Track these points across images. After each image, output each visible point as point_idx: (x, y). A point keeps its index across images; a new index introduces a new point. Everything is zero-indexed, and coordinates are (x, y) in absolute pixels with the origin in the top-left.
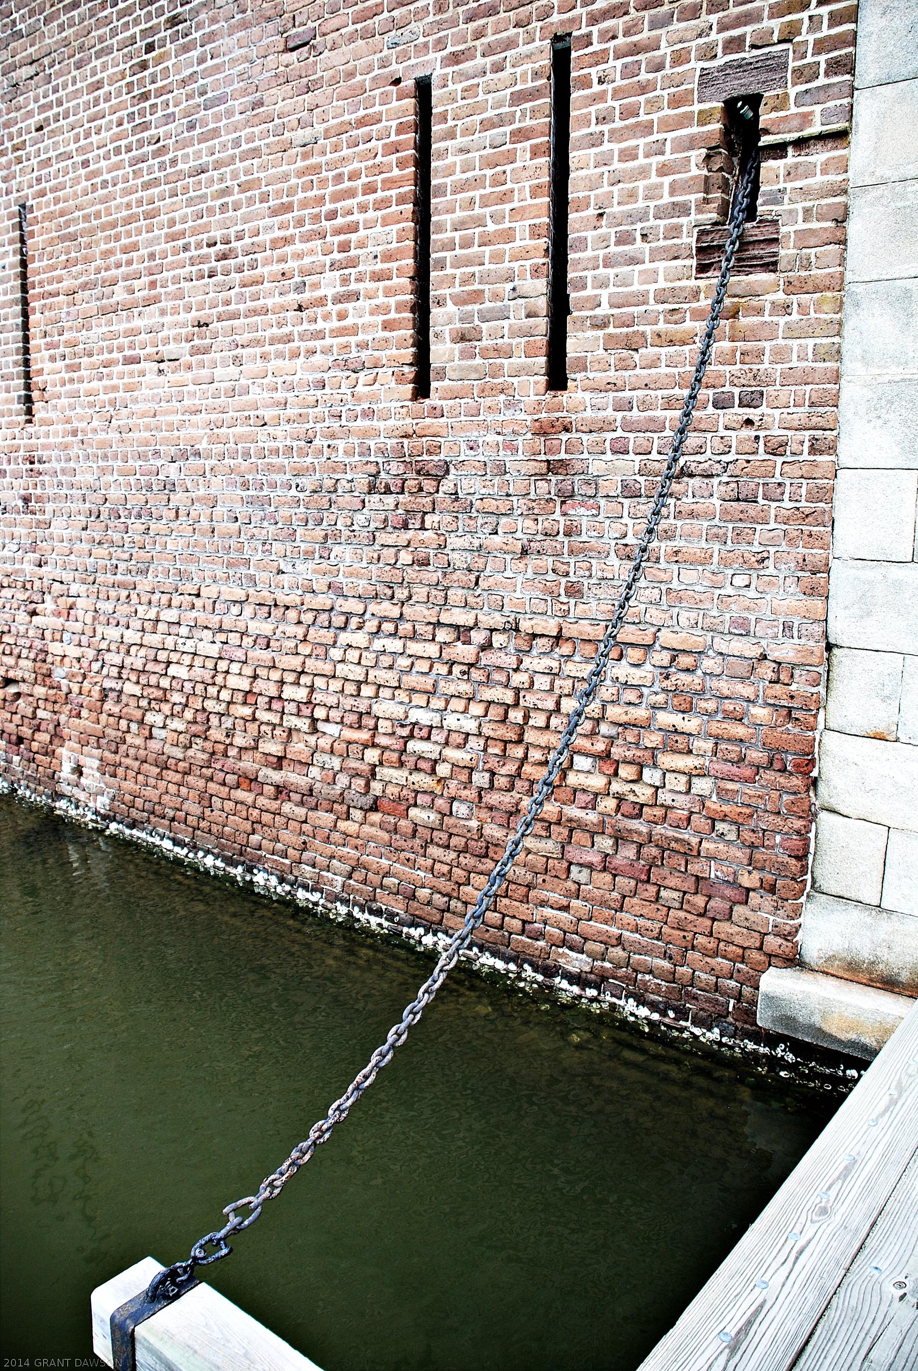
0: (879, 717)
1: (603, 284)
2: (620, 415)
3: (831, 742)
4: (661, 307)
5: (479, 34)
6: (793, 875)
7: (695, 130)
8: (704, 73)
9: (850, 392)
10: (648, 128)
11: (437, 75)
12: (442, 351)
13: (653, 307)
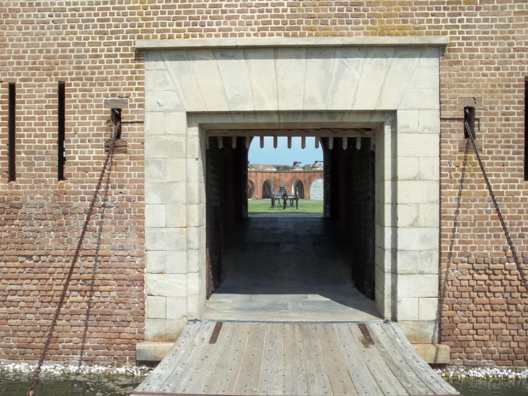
0: (160, 268)
2: (83, 190)
4: (94, 161)
5: (34, 75)
6: (140, 316)
7: (103, 115)
8: (106, 101)
9: (147, 185)
10: (89, 112)
11: (18, 82)
12: (20, 168)
13: (92, 160)
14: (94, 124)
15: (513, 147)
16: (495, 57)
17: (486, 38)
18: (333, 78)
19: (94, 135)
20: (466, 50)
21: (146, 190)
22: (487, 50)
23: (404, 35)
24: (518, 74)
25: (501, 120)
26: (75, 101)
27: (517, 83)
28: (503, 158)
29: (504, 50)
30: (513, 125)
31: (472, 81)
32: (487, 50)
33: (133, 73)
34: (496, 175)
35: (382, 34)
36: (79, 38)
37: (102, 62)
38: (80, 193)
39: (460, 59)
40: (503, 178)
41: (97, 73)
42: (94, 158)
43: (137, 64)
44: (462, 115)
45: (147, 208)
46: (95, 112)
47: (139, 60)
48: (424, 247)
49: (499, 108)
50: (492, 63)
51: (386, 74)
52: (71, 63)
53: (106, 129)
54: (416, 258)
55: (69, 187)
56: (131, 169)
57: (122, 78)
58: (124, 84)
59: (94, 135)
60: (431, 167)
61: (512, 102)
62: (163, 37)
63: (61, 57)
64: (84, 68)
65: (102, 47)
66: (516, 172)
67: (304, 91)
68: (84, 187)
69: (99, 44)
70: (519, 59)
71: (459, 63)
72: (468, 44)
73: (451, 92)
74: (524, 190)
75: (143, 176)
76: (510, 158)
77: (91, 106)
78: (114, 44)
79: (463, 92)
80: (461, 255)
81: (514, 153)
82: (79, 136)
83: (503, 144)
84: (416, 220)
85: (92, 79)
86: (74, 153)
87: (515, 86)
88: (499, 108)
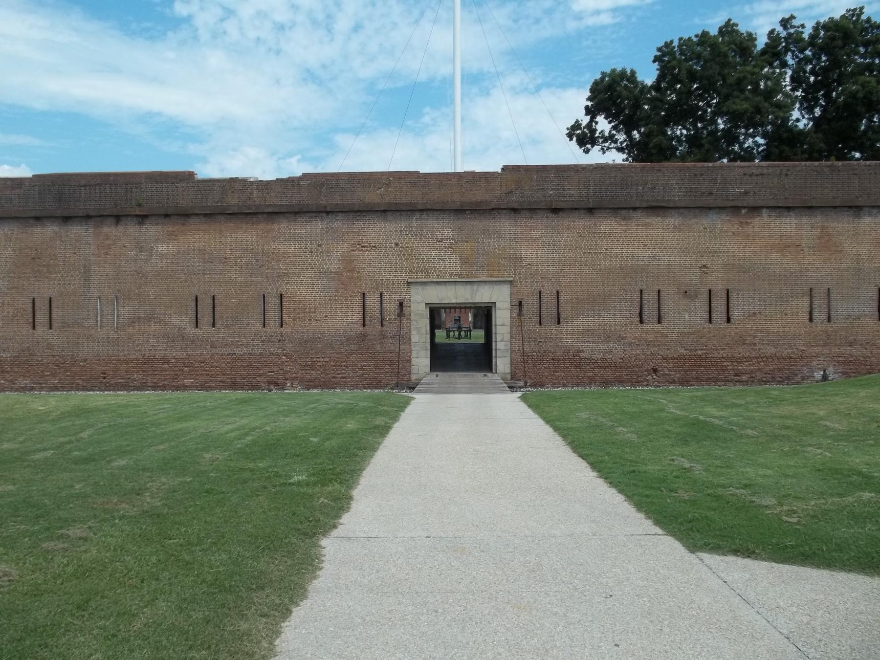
6: (410, 373)
12: (367, 322)
60: (508, 321)
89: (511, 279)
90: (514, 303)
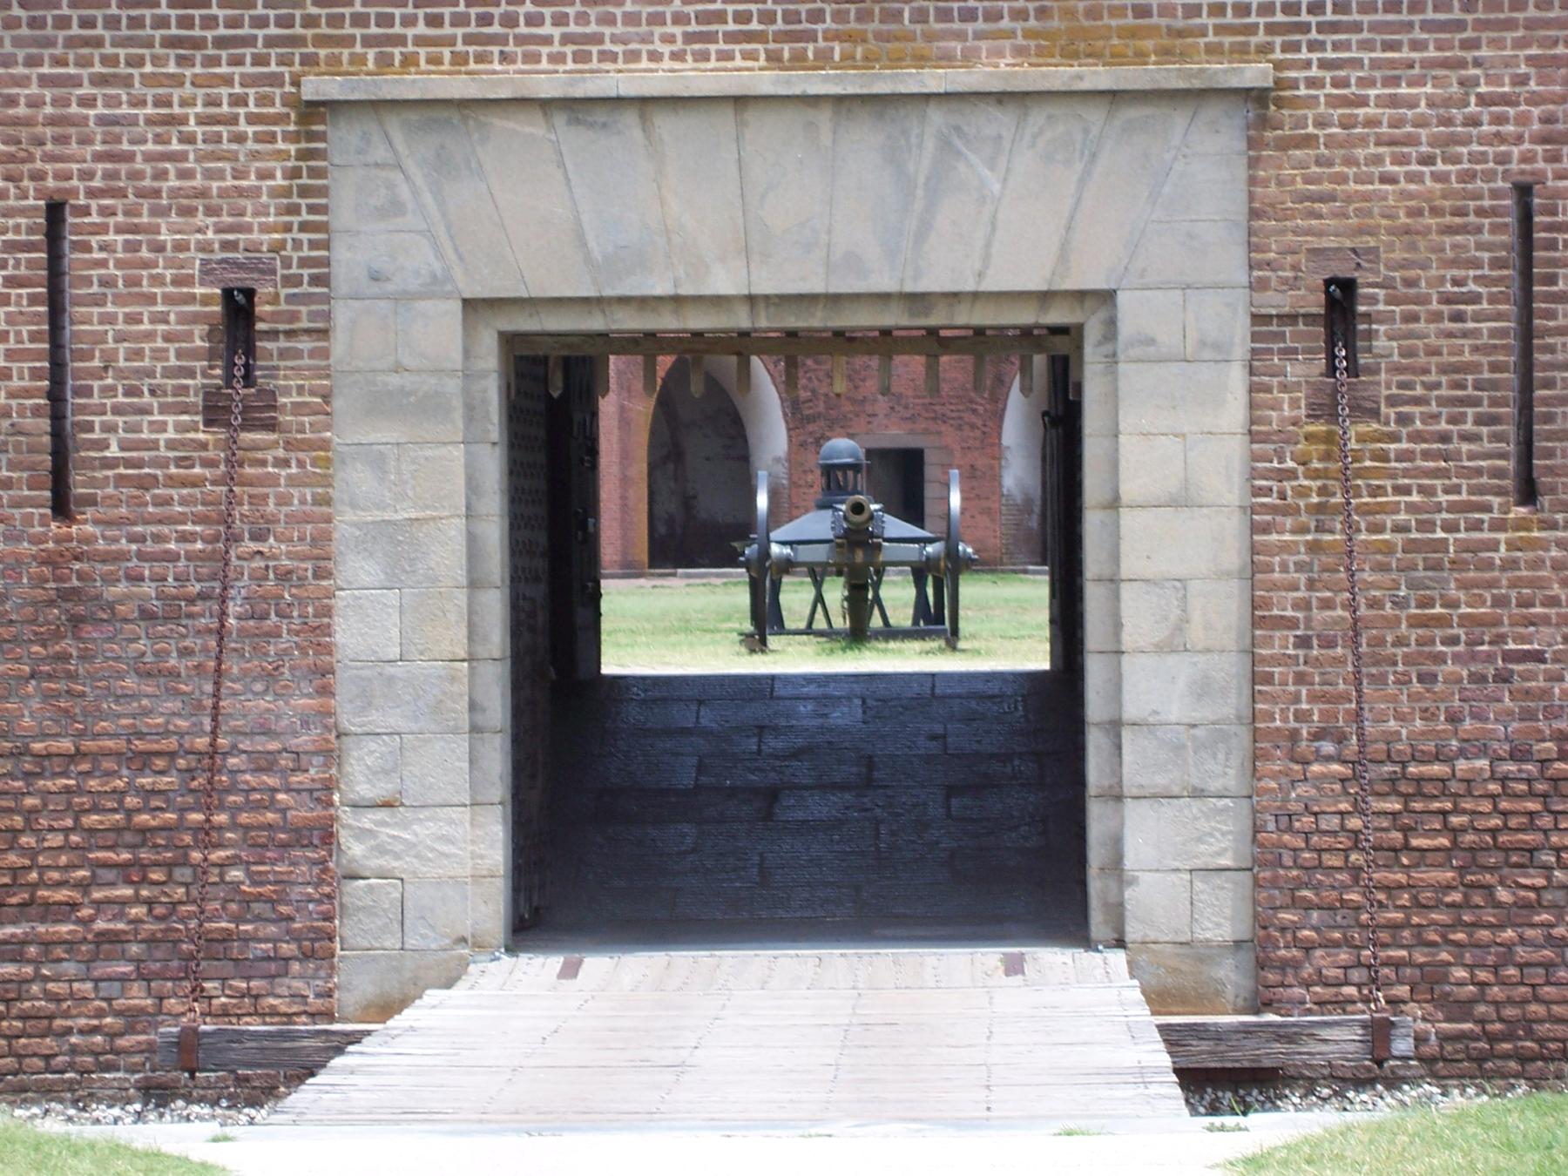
1: (110, 428)
2: (134, 547)
3: (346, 815)
4: (171, 454)
7: (197, 308)
8: (204, 262)
10: (150, 299)
13: (163, 452)
14: (168, 338)
15: (1476, 402)
16: (1421, 123)
17: (1392, 64)
18: (920, 192)
19: (169, 373)
20: (1334, 102)
21: (335, 547)
22: (1394, 102)
23: (1141, 57)
24: (1489, 176)
25: (1436, 317)
26: (103, 264)
27: (1487, 203)
28: (1445, 438)
29: (1448, 102)
30: (1475, 333)
31: (1349, 199)
32: (1394, 102)
33: (294, 174)
34: (1422, 490)
35: (1071, 55)
36: (108, 60)
37: (189, 139)
38: (121, 556)
39: (1311, 130)
40: (1443, 498)
41: (172, 174)
42: (171, 445)
43: (304, 145)
44: (1315, 303)
45: (342, 599)
46: (169, 299)
47: (312, 137)
48: (1204, 713)
49: (1434, 280)
50: (1412, 141)
51: (1083, 180)
52: (85, 141)
53: (211, 355)
54: (1179, 748)
55: (89, 540)
56: (292, 481)
57: (255, 192)
58: (262, 211)
59: (169, 373)
61: (1476, 264)
62: (384, 62)
63: (52, 121)
64: (129, 157)
65: (188, 89)
66: (1484, 480)
67: (829, 232)
68: (141, 539)
69: (178, 81)
70: (1494, 128)
71: (1309, 141)
72: (1336, 83)
73: (1283, 232)
74: (1509, 535)
75: (327, 501)
76: (1466, 437)
77: (157, 280)
78: (227, 81)
79: (1320, 234)
80: (1317, 736)
81: (1480, 420)
82: (121, 374)
83: (1444, 392)
84: (1180, 627)
85: (157, 193)
86: (106, 432)
87: (1480, 212)
88: (1434, 280)
89: (1255, 73)
90: (1276, 301)
